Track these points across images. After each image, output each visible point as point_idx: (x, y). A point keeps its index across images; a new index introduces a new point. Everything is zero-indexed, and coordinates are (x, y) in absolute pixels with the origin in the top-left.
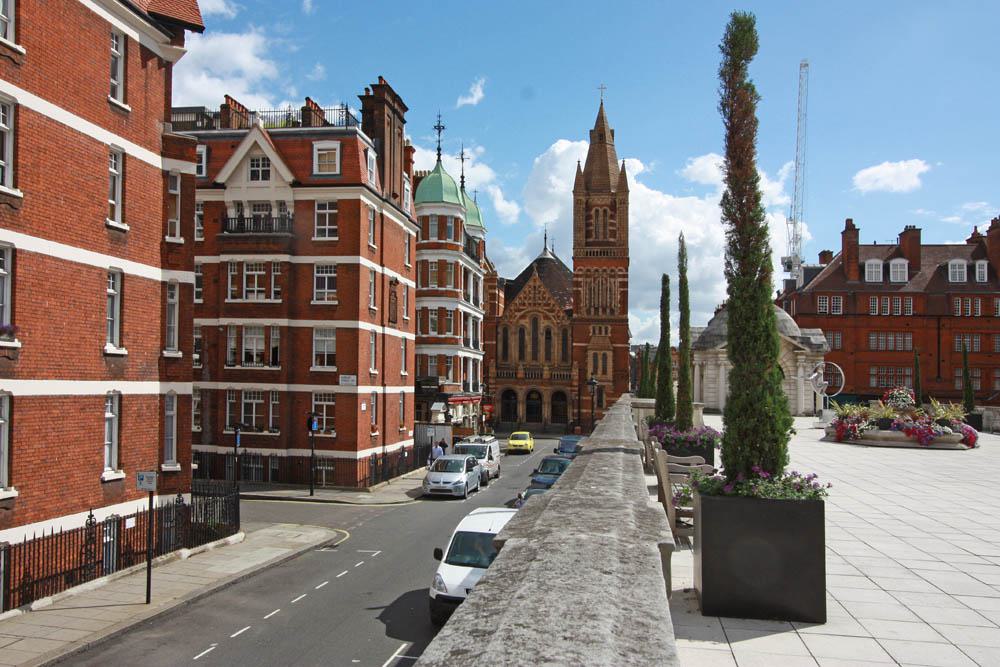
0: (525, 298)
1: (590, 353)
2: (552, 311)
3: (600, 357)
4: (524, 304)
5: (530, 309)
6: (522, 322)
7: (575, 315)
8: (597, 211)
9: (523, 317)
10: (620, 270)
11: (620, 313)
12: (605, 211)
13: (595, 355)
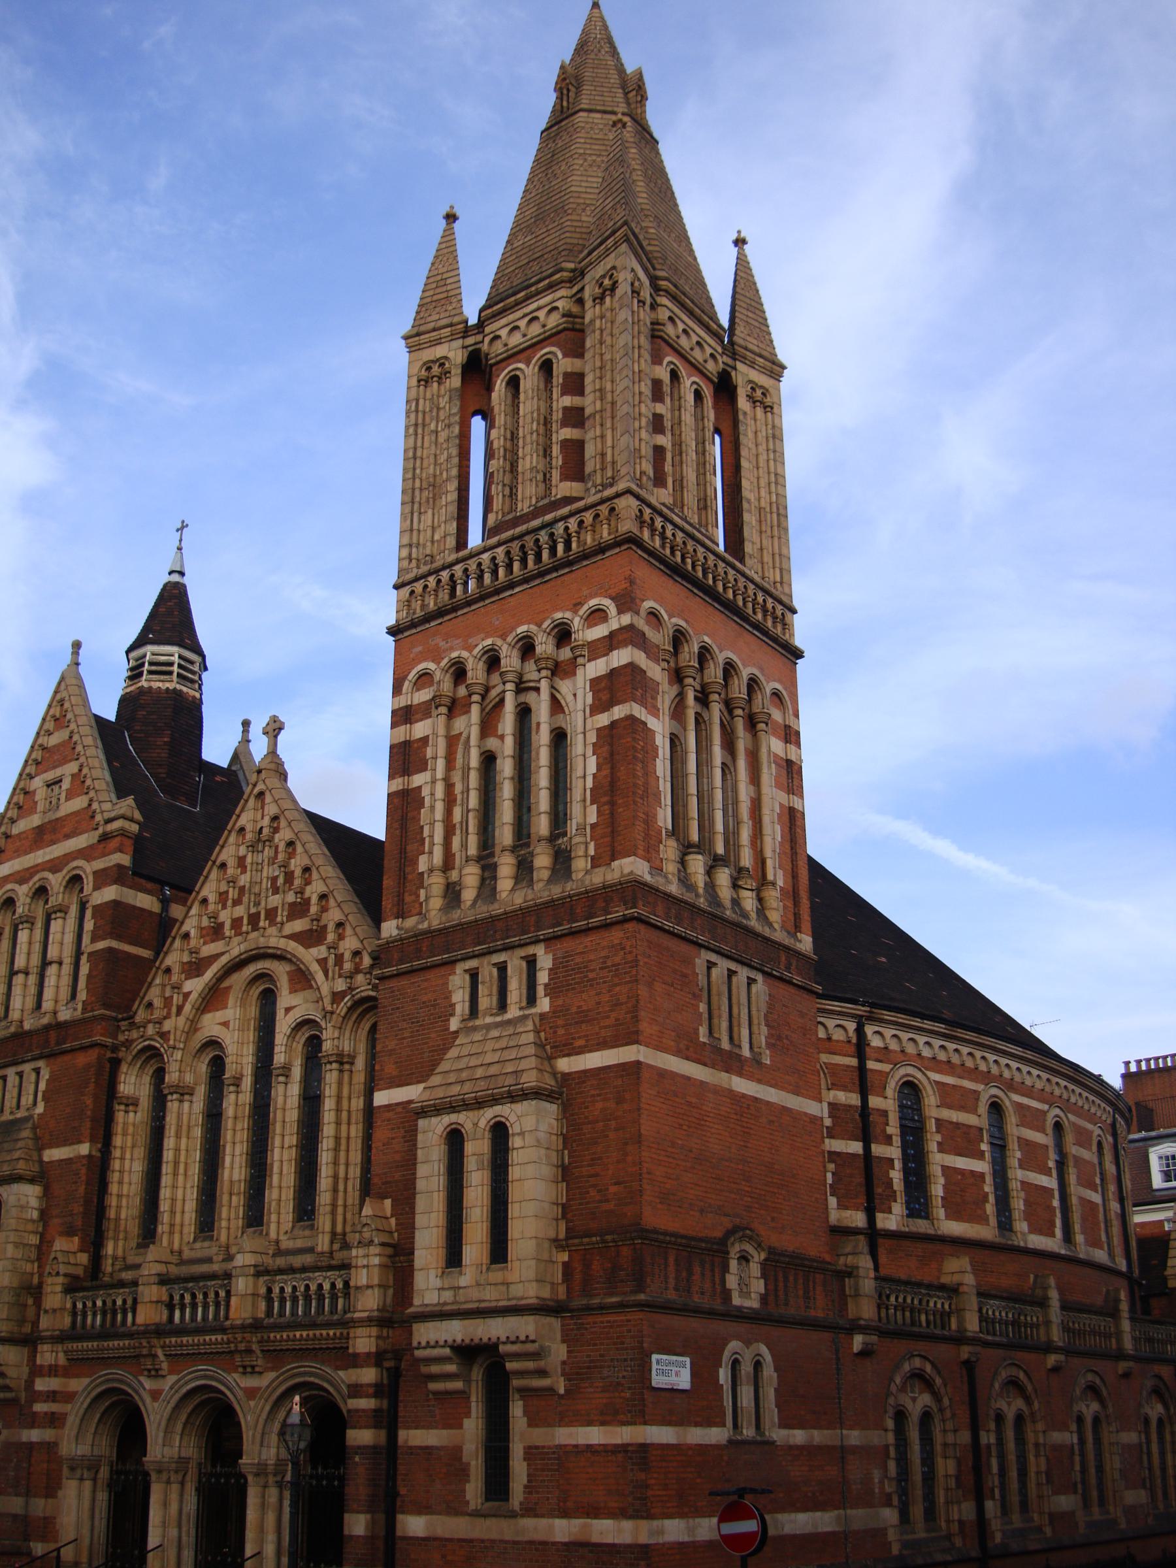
0: (223, 897)
1: (433, 1131)
2: (311, 938)
3: (477, 1149)
4: (215, 932)
5: (237, 948)
6: (211, 1025)
7: (390, 928)
8: (514, 383)
9: (213, 998)
10: (598, 615)
11: (596, 862)
12: (547, 367)
13: (455, 1139)
